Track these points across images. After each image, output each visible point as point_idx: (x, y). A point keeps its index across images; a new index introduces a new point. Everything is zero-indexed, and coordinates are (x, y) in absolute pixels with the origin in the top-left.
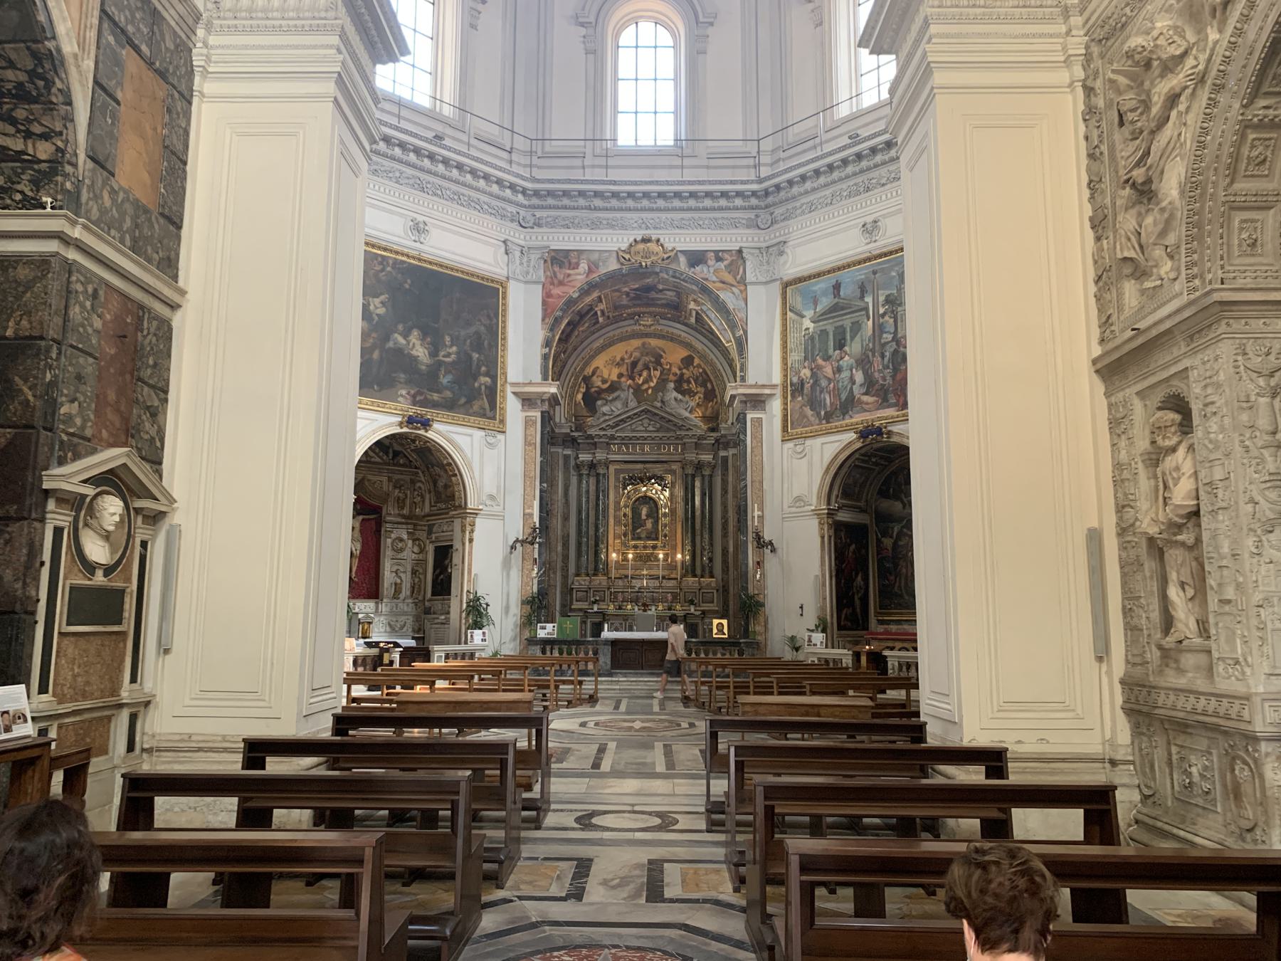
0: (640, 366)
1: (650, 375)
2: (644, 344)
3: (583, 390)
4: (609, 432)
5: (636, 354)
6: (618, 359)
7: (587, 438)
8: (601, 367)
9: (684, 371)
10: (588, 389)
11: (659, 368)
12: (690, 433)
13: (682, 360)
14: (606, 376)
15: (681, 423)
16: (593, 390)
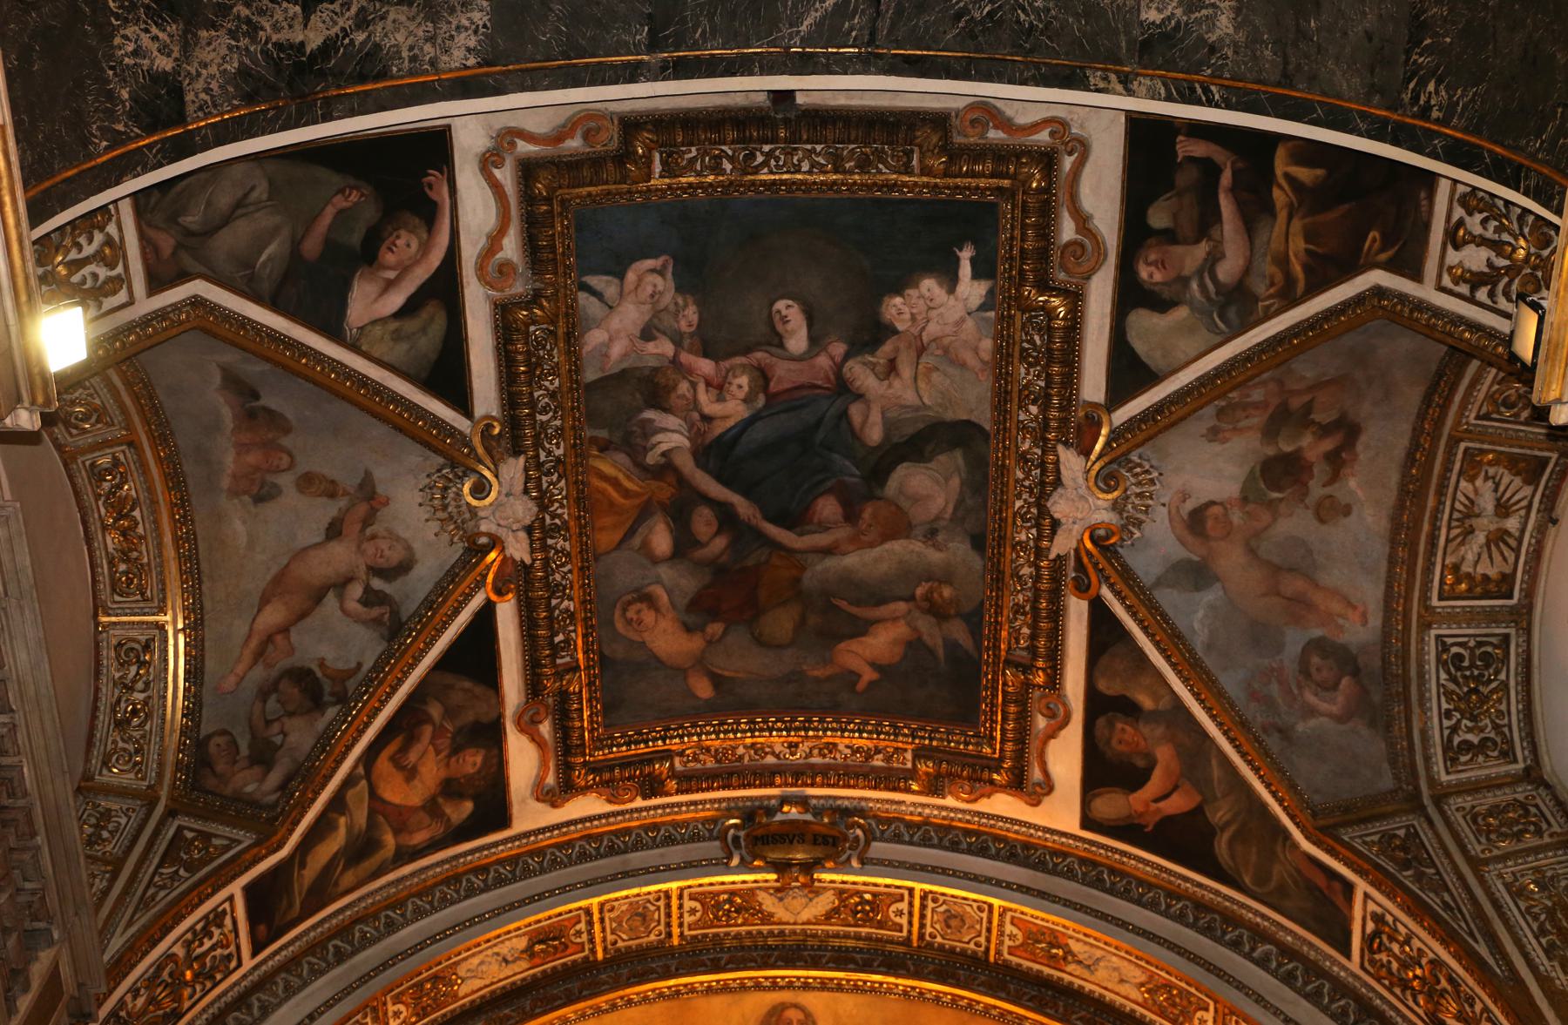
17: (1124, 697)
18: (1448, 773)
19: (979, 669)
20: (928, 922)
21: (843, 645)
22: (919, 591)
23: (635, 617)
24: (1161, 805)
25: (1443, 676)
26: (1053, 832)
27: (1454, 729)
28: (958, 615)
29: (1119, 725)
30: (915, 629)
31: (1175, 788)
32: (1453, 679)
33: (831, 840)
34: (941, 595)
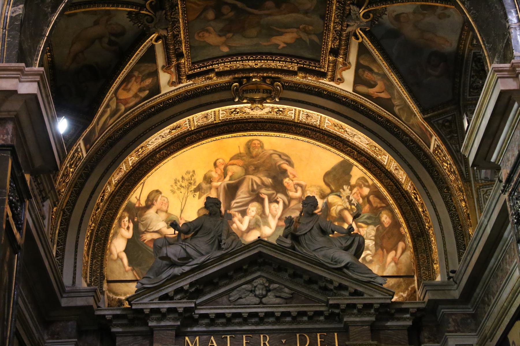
0: (242, 195)
1: (263, 214)
2: (249, 146)
3: (129, 234)
4: (181, 305)
5: (236, 170)
6: (199, 179)
7: (132, 323)
8: (166, 192)
9: (332, 198)
10: (137, 233)
11: (281, 197)
12: (359, 301)
13: (327, 175)
14: (175, 211)
15: (337, 280)
16: (148, 237)
17: (368, 66)
18: (469, 96)
19: (321, 47)
20: (301, 116)
21: (274, 37)
22: (301, 27)
23: (202, 35)
24: (379, 94)
25: (474, 64)
26: (343, 90)
27: (474, 82)
28: (314, 34)
29: (366, 72)
30: (299, 35)
31: (383, 92)
32: (476, 66)
33: (269, 91)
34: (309, 28)
